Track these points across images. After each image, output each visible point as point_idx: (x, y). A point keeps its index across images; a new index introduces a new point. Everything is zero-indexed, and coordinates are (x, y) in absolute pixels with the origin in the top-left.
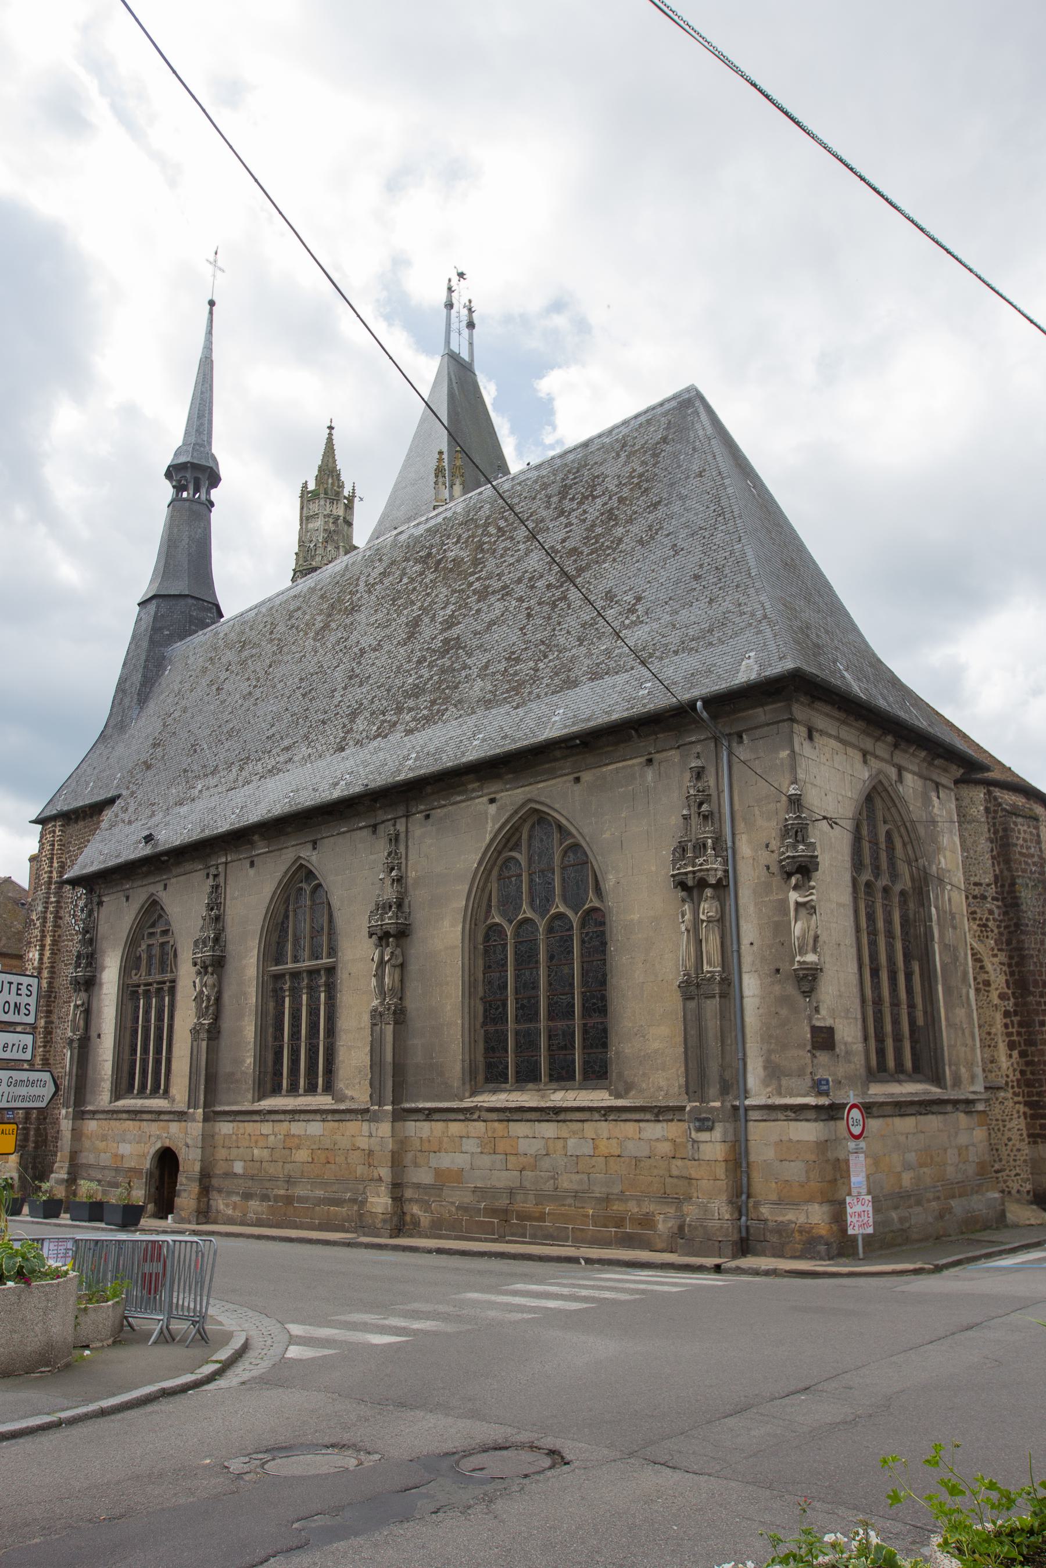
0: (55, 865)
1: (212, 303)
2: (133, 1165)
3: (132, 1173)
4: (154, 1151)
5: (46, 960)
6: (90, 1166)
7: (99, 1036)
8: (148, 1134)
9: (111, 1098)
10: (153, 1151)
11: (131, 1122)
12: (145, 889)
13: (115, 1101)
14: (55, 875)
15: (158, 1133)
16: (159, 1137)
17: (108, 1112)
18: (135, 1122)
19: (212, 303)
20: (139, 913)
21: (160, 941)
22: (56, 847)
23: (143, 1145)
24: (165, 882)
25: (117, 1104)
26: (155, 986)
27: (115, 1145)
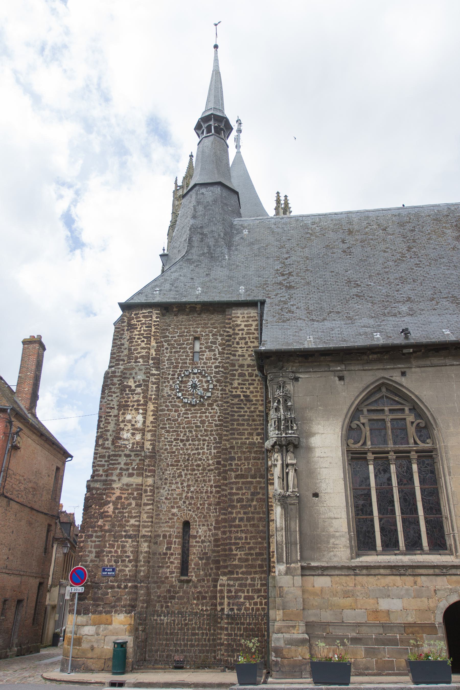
0: (153, 343)
1: (216, 47)
2: (410, 620)
3: (417, 629)
4: (447, 605)
5: (148, 423)
6: (328, 624)
7: (316, 495)
8: (432, 588)
9: (351, 554)
10: (444, 605)
11: (398, 578)
12: (370, 373)
13: (356, 558)
14: (153, 352)
15: (450, 587)
16: (452, 591)
17: (349, 568)
18: (403, 578)
19: (216, 47)
20: (363, 391)
21: (391, 417)
22: (153, 329)
23: (425, 600)
24: (403, 370)
25: (358, 560)
26: (391, 453)
27: (372, 601)
